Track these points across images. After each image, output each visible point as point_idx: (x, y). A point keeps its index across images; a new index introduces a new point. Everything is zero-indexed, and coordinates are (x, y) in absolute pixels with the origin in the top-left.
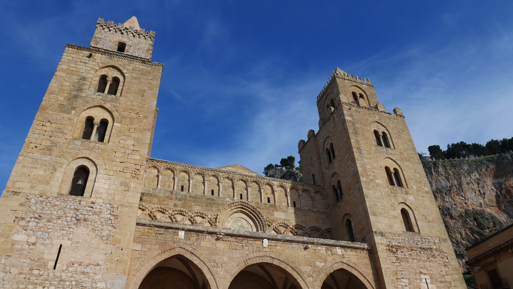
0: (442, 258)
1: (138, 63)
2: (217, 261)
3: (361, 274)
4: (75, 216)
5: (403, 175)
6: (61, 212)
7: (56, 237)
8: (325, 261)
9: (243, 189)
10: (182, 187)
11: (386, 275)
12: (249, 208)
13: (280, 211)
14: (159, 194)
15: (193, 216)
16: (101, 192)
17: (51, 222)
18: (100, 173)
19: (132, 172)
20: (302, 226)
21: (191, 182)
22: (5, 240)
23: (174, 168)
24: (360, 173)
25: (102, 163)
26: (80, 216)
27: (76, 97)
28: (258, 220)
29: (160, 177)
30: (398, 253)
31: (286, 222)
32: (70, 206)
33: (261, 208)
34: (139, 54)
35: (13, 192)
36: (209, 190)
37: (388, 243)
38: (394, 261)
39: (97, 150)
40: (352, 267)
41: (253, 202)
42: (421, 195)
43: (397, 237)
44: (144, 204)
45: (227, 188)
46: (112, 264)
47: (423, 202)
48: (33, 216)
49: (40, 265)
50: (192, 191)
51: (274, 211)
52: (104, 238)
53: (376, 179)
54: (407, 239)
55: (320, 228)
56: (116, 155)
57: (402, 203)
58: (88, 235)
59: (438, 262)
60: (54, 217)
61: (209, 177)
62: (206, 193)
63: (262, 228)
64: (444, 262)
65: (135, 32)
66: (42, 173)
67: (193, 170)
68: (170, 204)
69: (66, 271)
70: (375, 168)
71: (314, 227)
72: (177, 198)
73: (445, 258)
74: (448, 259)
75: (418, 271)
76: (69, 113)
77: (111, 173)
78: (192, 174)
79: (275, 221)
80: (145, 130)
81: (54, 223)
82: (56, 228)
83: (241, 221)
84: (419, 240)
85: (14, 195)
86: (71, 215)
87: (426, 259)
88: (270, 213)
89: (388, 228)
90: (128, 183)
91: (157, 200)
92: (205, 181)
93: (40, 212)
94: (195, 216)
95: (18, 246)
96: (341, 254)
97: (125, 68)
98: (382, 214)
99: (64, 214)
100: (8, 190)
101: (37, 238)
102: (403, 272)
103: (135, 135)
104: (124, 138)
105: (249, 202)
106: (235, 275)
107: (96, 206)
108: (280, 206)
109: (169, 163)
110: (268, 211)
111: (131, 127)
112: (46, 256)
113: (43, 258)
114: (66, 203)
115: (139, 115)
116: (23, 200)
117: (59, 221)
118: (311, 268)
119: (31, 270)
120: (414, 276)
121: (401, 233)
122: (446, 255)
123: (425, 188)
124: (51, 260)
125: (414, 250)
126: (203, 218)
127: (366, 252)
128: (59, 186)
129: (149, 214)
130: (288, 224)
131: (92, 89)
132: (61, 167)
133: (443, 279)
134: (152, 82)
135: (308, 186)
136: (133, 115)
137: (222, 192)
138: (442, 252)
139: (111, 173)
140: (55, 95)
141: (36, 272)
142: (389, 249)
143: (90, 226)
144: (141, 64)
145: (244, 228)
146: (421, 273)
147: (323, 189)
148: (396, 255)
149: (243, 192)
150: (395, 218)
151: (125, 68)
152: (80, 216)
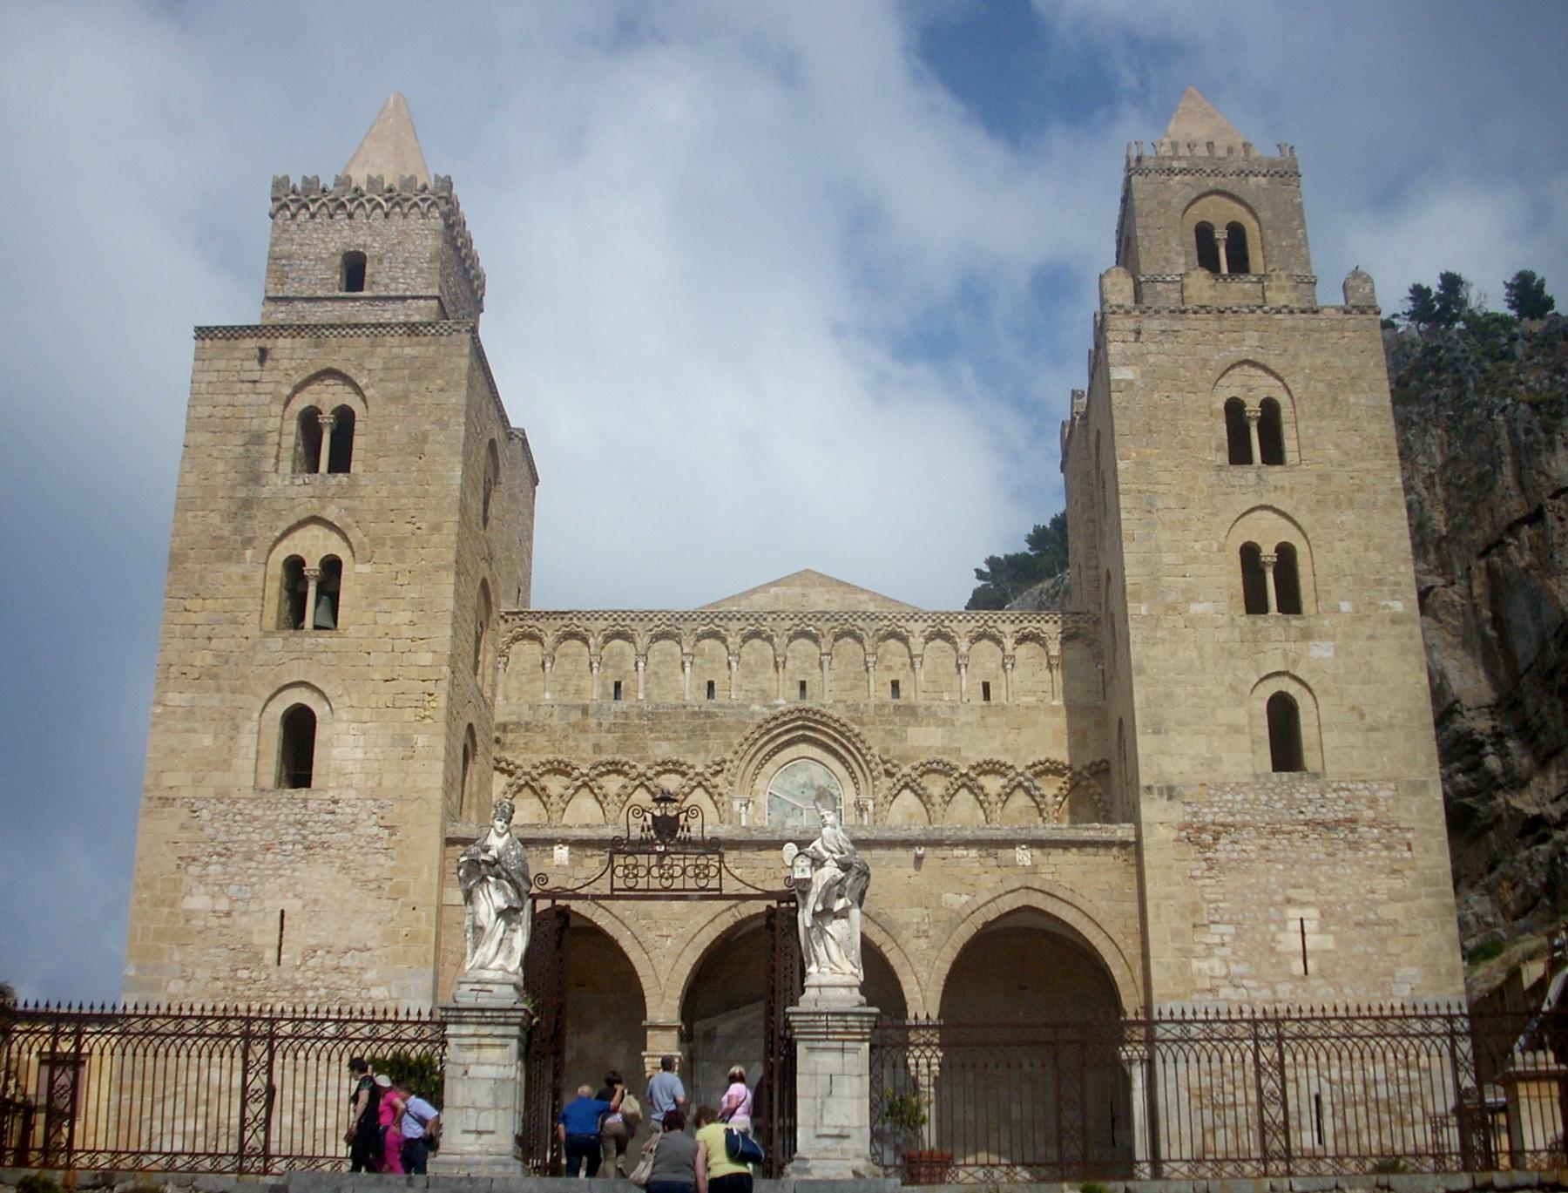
0: (1388, 847)
1: (396, 341)
2: (656, 917)
11: (1158, 916)
16: (350, 769)
17: (251, 859)
18: (340, 720)
19: (415, 704)
24: (1129, 589)
25: (340, 692)
30: (1218, 847)
32: (287, 816)
35: (160, 798)
38: (1198, 873)
40: (1062, 900)
43: (1229, 797)
46: (397, 943)
47: (1368, 658)
49: (248, 960)
52: (372, 886)
54: (1264, 798)
56: (372, 659)
57: (1278, 674)
58: (336, 881)
59: (1368, 863)
64: (1394, 860)
65: (387, 195)
66: (207, 740)
70: (1195, 559)
73: (1398, 846)
74: (1410, 849)
75: (1279, 898)
76: (240, 560)
80: (437, 569)
81: (260, 863)
82: (266, 872)
85: (164, 806)
86: (290, 838)
87: (1322, 856)
89: (1201, 769)
93: (225, 839)
95: (198, 923)
96: (1029, 863)
97: (361, 368)
98: (1188, 724)
99: (276, 836)
100: (150, 795)
101: (232, 901)
102: (1221, 905)
104: (385, 605)
106: (705, 946)
111: (399, 566)
112: (257, 939)
113: (250, 943)
114: (276, 809)
115: (418, 525)
116: (185, 811)
117: (269, 857)
118: (926, 912)
120: (1259, 916)
122: (1409, 836)
123: (1391, 604)
125: (1284, 833)
131: (286, 467)
132: (249, 718)
133: (1371, 916)
134: (443, 396)
141: (244, 974)
144: (406, 340)
146: (1289, 901)
148: (1208, 855)
150: (1235, 732)
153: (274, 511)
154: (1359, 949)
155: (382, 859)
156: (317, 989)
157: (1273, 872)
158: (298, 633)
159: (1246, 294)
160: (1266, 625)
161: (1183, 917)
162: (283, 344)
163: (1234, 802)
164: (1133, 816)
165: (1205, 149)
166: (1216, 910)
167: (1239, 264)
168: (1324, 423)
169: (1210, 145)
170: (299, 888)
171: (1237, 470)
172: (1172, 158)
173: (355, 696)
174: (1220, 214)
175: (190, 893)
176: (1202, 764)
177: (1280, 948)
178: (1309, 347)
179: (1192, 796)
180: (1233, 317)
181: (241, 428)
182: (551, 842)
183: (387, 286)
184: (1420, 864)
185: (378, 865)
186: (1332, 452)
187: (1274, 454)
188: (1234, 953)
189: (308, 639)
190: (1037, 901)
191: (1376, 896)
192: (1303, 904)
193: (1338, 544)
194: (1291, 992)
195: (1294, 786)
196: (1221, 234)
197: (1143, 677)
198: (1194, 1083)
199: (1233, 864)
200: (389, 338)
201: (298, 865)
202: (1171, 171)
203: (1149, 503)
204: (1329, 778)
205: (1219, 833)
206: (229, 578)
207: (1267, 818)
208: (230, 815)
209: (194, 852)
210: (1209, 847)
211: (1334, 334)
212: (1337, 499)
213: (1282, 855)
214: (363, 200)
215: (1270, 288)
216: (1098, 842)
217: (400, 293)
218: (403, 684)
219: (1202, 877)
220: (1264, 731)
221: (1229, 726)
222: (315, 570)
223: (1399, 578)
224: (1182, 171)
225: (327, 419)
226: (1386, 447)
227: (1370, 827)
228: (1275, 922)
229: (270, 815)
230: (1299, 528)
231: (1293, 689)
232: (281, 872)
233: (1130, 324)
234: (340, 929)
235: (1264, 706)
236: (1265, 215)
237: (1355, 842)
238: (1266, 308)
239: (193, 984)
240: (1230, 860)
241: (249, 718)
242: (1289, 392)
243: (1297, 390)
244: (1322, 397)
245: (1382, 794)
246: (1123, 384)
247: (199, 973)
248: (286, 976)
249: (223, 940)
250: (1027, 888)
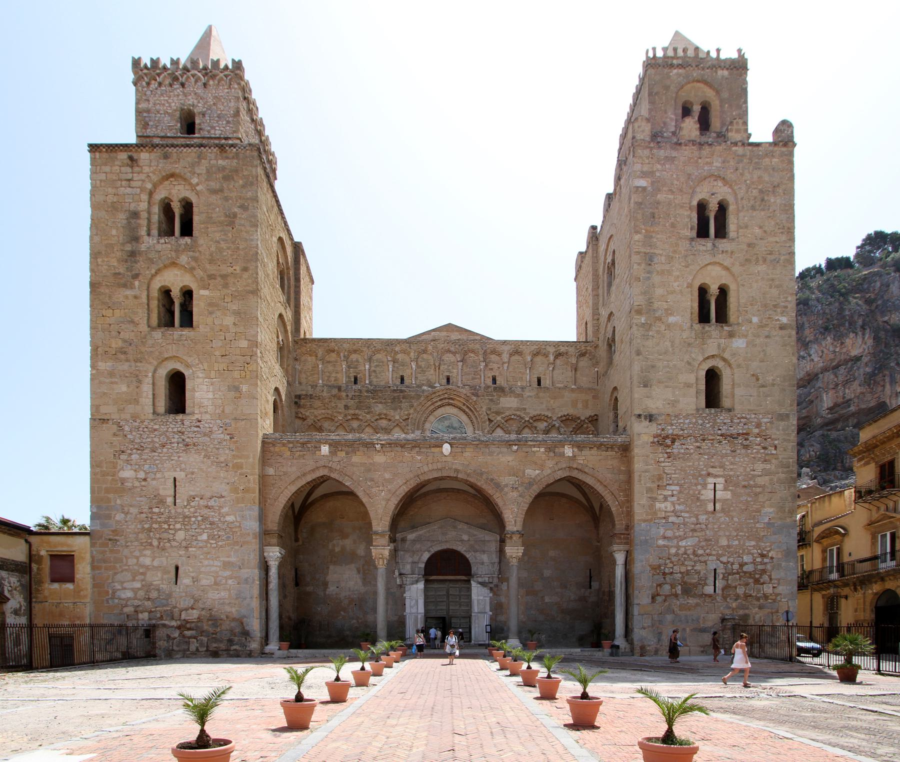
0: (765, 448)
8: (542, 467)
18: (198, 377)
19: (239, 368)
25: (197, 362)
27: (133, 254)
32: (172, 428)
52: (223, 465)
54: (700, 422)
58: (203, 462)
60: (157, 445)
64: (767, 454)
85: (103, 423)
86: (176, 440)
87: (729, 452)
89: (667, 406)
93: (139, 441)
101: (146, 473)
112: (162, 492)
116: (115, 426)
117: (165, 450)
122: (776, 442)
124: (169, 496)
148: (668, 451)
150: (688, 387)
163: (684, 423)
175: (122, 469)
184: (780, 457)
185: (225, 455)
190: (575, 474)
195: (717, 416)
199: (681, 455)
201: (181, 455)
204: (736, 412)
209: (123, 448)
210: (668, 446)
213: (707, 451)
219: (664, 462)
221: (686, 383)
227: (756, 437)
229: (163, 428)
245: (765, 420)
248: (180, 510)
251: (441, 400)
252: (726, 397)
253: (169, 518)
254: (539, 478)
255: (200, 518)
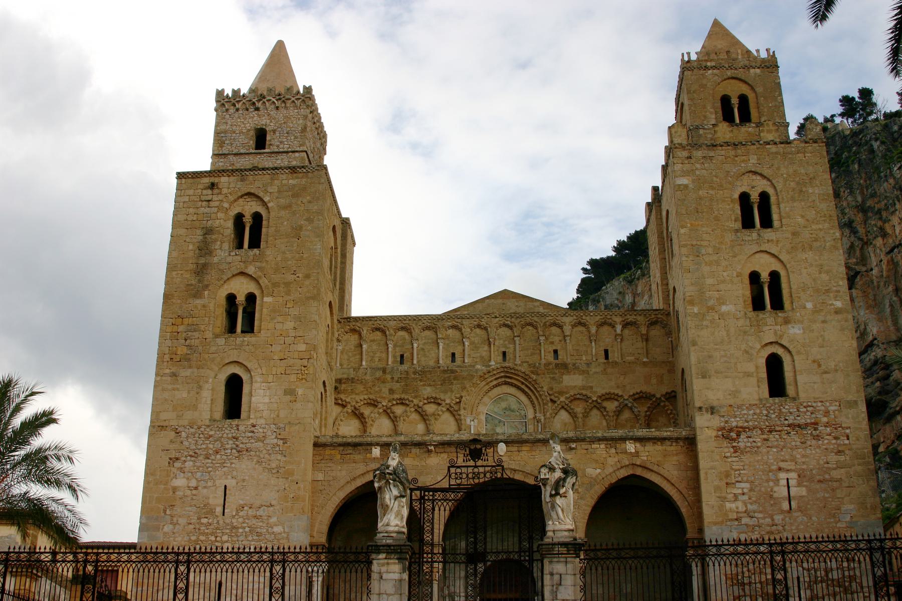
0: (836, 438)
1: (284, 177)
3: (668, 480)
4: (234, 446)
5: (789, 282)
6: (218, 444)
7: (218, 477)
9: (507, 342)
10: (402, 356)
11: (706, 479)
12: (519, 376)
13: (574, 374)
14: (365, 377)
15: (421, 404)
17: (208, 458)
18: (256, 382)
19: (297, 372)
20: (617, 395)
21: (415, 345)
22: (165, 488)
23: (384, 326)
25: (256, 367)
26: (241, 446)
28: (535, 395)
29: (365, 346)
30: (740, 440)
31: (584, 392)
32: (227, 434)
33: (540, 372)
34: (290, 143)
35: (159, 427)
36: (447, 355)
37: (722, 424)
38: (728, 454)
39: (247, 347)
41: (525, 364)
42: (821, 318)
43: (745, 412)
44: (343, 396)
45: (478, 345)
46: (288, 502)
47: (822, 333)
48: (187, 454)
49: (207, 513)
50: (418, 362)
51: (563, 374)
52: (274, 471)
53: (723, 304)
54: (765, 412)
55: (653, 393)
56: (273, 349)
57: (771, 343)
58: (254, 469)
60: (211, 452)
61: (446, 330)
62: (441, 362)
63: (542, 408)
64: (839, 445)
65: (278, 97)
66: (185, 395)
67: (416, 324)
68: (384, 390)
69: (236, 517)
70: (723, 282)
71: (641, 392)
72: (392, 378)
73: (842, 438)
74: (848, 439)
75: (774, 467)
77: (270, 379)
78: (417, 331)
79: (564, 392)
80: (308, 299)
81: (213, 460)
83: (507, 400)
84: (791, 410)
85: (161, 430)
86: (230, 446)
87: (798, 443)
88: (556, 380)
89: (729, 397)
90: (294, 390)
91: (363, 386)
92: (439, 341)
94: (425, 404)
95: (179, 494)
96: (633, 451)
97: (266, 191)
98: (722, 372)
101: (198, 481)
102: (742, 472)
103: (295, 312)
104: (280, 319)
105: (516, 365)
107: (258, 429)
108: (574, 365)
109: (376, 319)
110: (552, 376)
111: (288, 298)
112: (211, 501)
113: (208, 504)
114: (222, 430)
115: (297, 275)
117: (218, 456)
119: (199, 519)
120: (763, 477)
121: (754, 403)
122: (848, 431)
123: (834, 303)
124: (218, 506)
125: (776, 431)
126: (439, 404)
127: (684, 443)
128: (209, 409)
129: (353, 411)
130: (590, 395)
131: (226, 246)
132: (207, 382)
133: (827, 476)
135: (635, 315)
136: (291, 278)
137: (469, 355)
138: (839, 427)
139: (270, 379)
140: (179, 272)
141: (204, 521)
142: (723, 435)
143: (255, 457)
145: (513, 411)
146: (780, 469)
147: (666, 314)
148: (734, 444)
149: (508, 348)
150: (748, 376)
151: (266, 191)
152: (241, 446)
153: (220, 270)
154: (820, 495)
155: (279, 457)
156: (244, 528)
157: (771, 453)
158: (233, 335)
159: (749, 134)
160: (764, 316)
161: (721, 479)
162: (224, 180)
164: (690, 424)
165: (725, 54)
166: (739, 475)
167: (746, 118)
168: (795, 204)
169: (728, 52)
170: (235, 473)
171: (747, 232)
172: (706, 61)
173: (264, 369)
174: (734, 90)
176: (730, 394)
177: (775, 495)
178: (786, 163)
179: (724, 412)
180: (743, 148)
181: (202, 226)
182: (371, 444)
183: (278, 146)
186: (800, 220)
187: (767, 222)
188: (750, 499)
189: (240, 339)
190: (639, 472)
191: (830, 465)
192: (788, 471)
193: (804, 271)
194: (782, 520)
196: (735, 101)
197: (696, 347)
198: (729, 572)
199: (748, 449)
200: (281, 176)
201: (234, 461)
202: (706, 68)
203: (697, 252)
205: (740, 432)
206: (196, 307)
207: (767, 424)
208: (197, 435)
209: (178, 455)
211: (800, 155)
212: (803, 245)
213: (776, 443)
214: (265, 100)
215: (763, 131)
216: (672, 438)
217: (286, 150)
218: (291, 362)
219: (731, 457)
220: (764, 375)
222: (242, 301)
223: (839, 288)
224: (713, 68)
225: (248, 220)
226: (830, 216)
228: (772, 481)
229: (219, 434)
230: (782, 262)
231: (780, 351)
232: (225, 465)
233: (685, 154)
234: (257, 495)
235: (764, 361)
236: (759, 90)
237: (818, 436)
238: (761, 142)
239: (177, 526)
240: (746, 447)
241: (207, 382)
242: (775, 188)
243: (779, 187)
244: (794, 190)
246: (682, 187)
247: (182, 521)
248: (228, 521)
249: (194, 502)
250: (633, 464)
251: (496, 379)
252: (790, 385)
253: (217, 529)
254: (601, 478)
255: (247, 529)
